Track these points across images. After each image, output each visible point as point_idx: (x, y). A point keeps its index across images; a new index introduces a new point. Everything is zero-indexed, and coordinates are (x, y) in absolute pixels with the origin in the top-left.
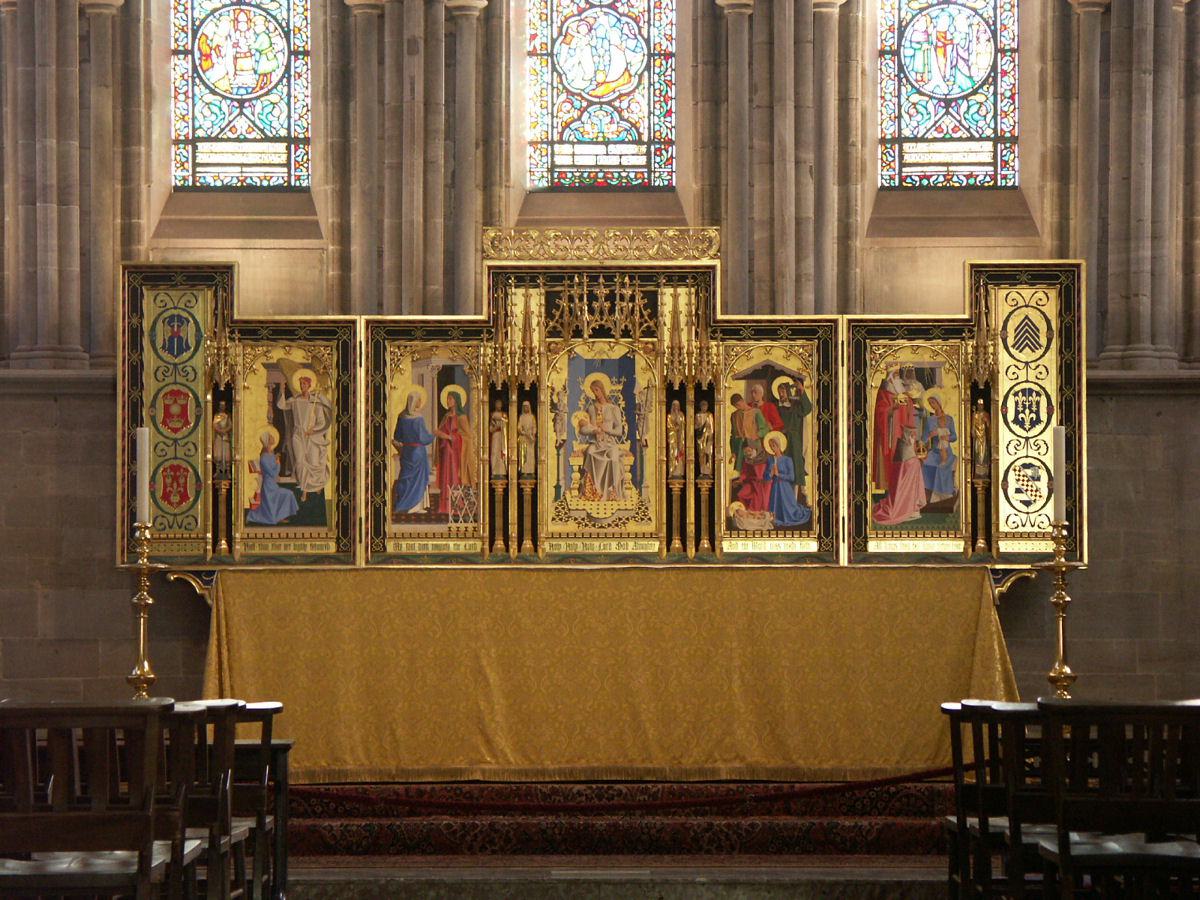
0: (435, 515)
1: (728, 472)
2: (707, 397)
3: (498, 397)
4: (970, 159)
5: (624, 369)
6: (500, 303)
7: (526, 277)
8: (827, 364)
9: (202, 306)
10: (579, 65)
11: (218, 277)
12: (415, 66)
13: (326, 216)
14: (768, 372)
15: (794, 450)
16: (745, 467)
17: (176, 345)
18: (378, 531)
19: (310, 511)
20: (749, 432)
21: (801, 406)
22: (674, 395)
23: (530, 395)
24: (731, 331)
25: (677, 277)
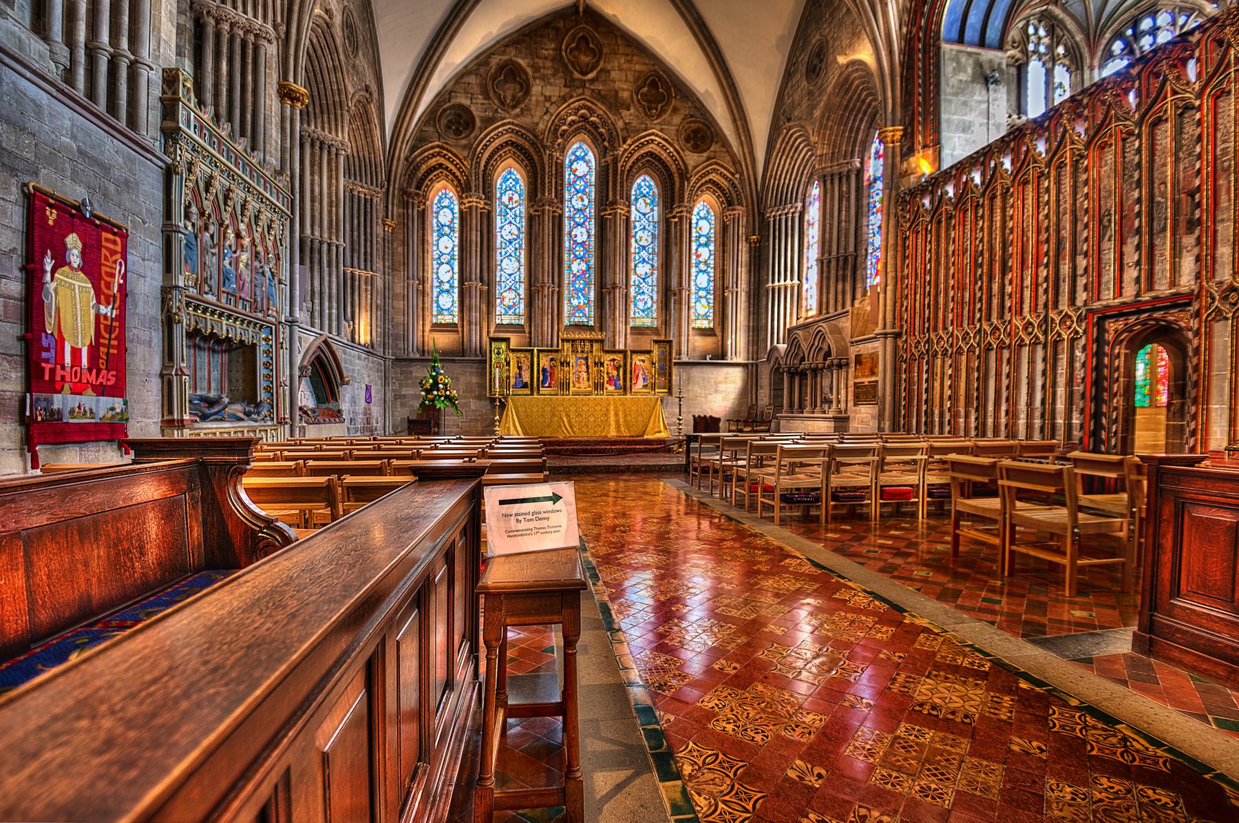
0: (549, 387)
1: (606, 379)
2: (602, 364)
3: (562, 364)
4: (648, 322)
5: (586, 359)
6: (563, 346)
7: (568, 341)
8: (625, 358)
9: (503, 346)
10: (575, 302)
11: (507, 340)
12: (546, 300)
13: (527, 330)
14: (613, 360)
15: (618, 375)
16: (610, 378)
17: (499, 353)
18: (538, 389)
19: (525, 386)
20: (610, 371)
21: (620, 366)
22: (596, 364)
23: (568, 364)
24: (607, 352)
25: (597, 341)
